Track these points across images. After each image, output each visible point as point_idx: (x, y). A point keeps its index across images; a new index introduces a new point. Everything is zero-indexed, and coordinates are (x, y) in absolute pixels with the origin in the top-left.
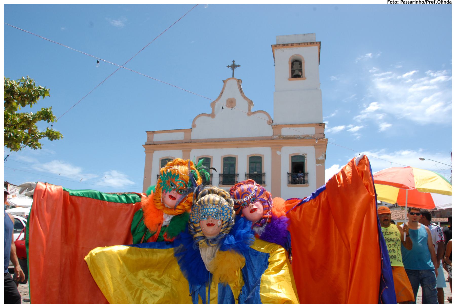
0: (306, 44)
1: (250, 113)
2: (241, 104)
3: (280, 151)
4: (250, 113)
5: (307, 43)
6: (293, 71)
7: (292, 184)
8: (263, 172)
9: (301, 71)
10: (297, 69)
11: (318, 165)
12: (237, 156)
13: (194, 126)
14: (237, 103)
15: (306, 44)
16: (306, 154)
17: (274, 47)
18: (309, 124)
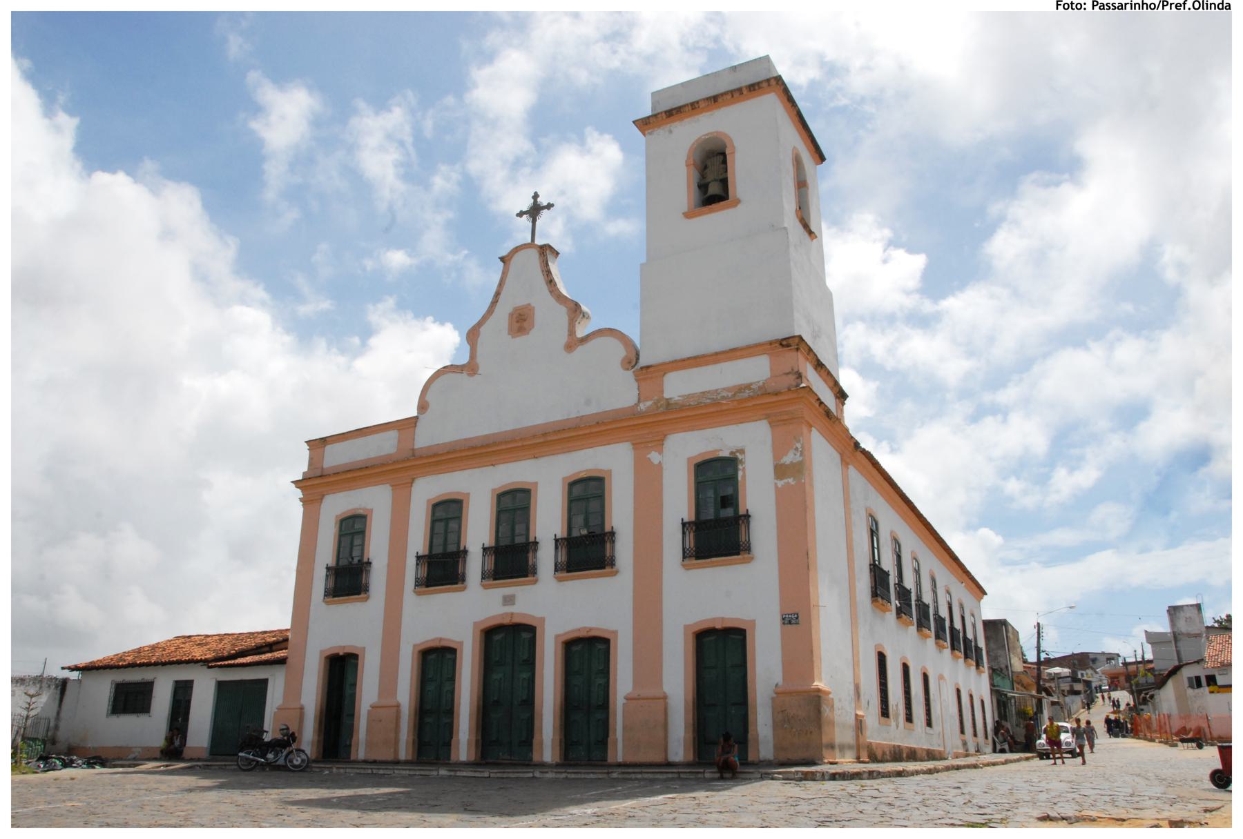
0: (736, 95)
1: (573, 343)
2: (550, 319)
3: (661, 452)
4: (573, 343)
5: (740, 90)
6: (703, 187)
7: (697, 558)
8: (607, 529)
9: (724, 182)
10: (712, 182)
11: (780, 483)
12: (610, 472)
13: (423, 406)
14: (539, 317)
15: (736, 95)
16: (742, 451)
17: (644, 124)
18: (749, 347)
